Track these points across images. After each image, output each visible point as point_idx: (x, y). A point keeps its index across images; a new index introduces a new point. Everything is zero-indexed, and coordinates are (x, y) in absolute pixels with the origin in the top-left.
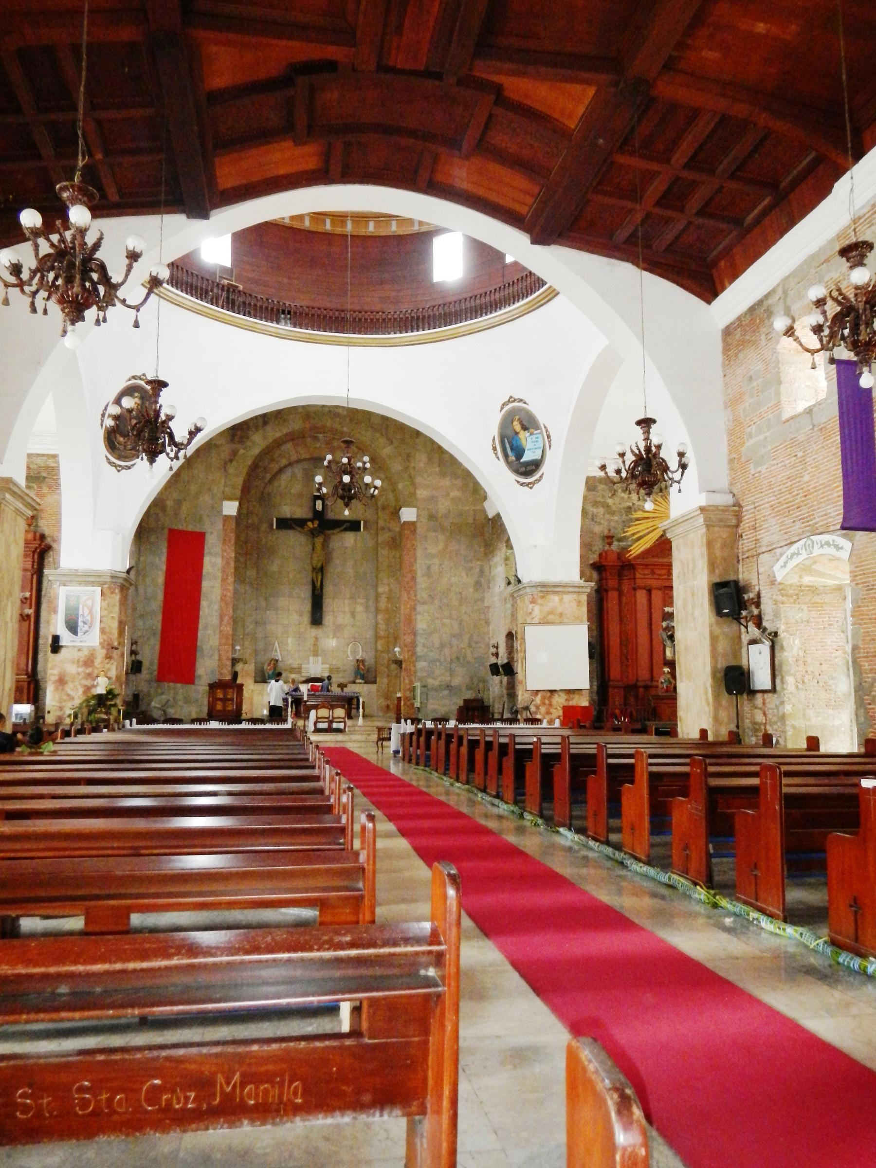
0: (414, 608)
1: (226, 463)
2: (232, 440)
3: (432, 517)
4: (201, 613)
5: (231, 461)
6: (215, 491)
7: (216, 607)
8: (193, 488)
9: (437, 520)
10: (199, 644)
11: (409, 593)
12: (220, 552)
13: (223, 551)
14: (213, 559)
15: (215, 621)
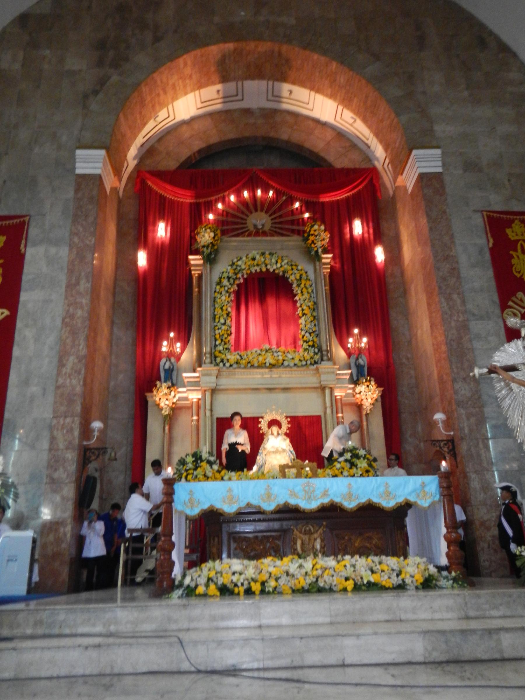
0: (464, 327)
1: (86, 97)
2: (100, 63)
3: (471, 166)
4: (16, 352)
5: (96, 93)
6: (64, 138)
7: (51, 339)
8: (24, 135)
9: (480, 170)
10: (7, 415)
11: (449, 298)
12: (67, 235)
13: (73, 234)
14: (53, 250)
15: (46, 365)
